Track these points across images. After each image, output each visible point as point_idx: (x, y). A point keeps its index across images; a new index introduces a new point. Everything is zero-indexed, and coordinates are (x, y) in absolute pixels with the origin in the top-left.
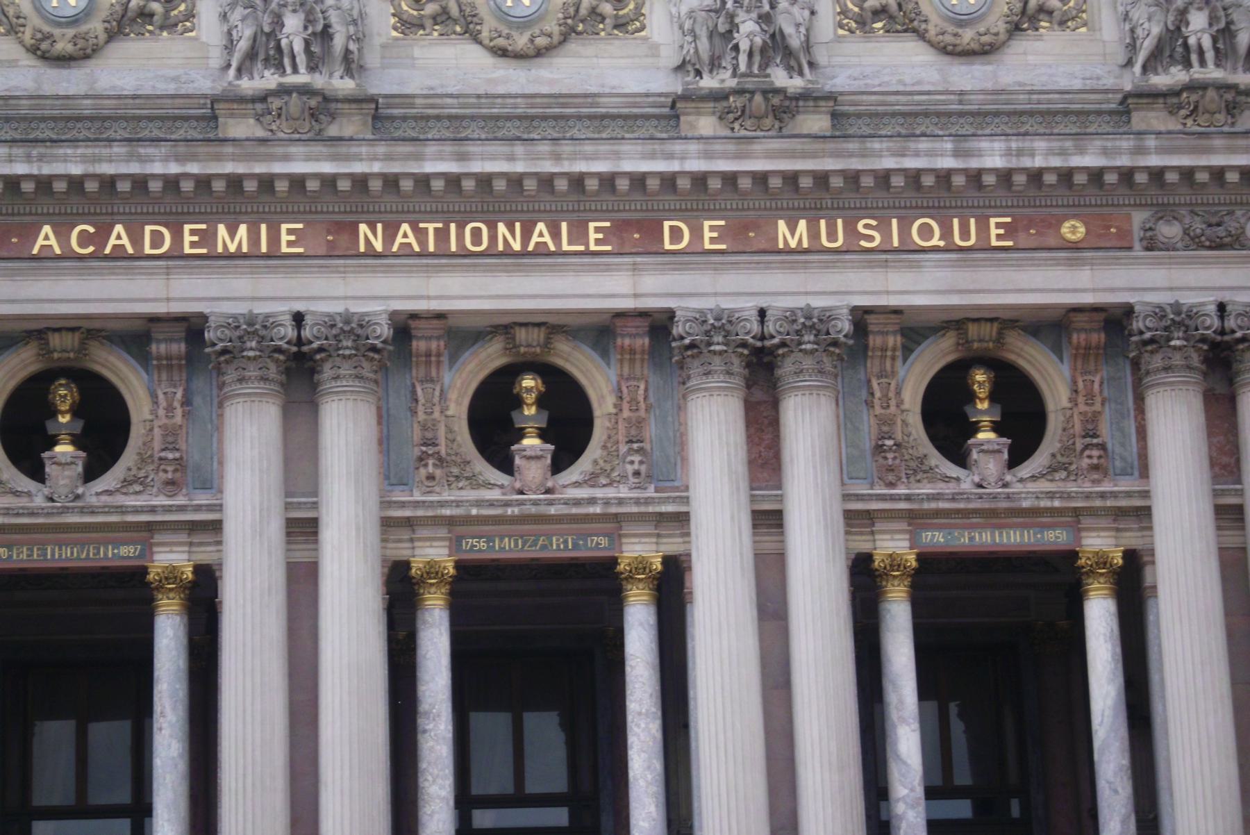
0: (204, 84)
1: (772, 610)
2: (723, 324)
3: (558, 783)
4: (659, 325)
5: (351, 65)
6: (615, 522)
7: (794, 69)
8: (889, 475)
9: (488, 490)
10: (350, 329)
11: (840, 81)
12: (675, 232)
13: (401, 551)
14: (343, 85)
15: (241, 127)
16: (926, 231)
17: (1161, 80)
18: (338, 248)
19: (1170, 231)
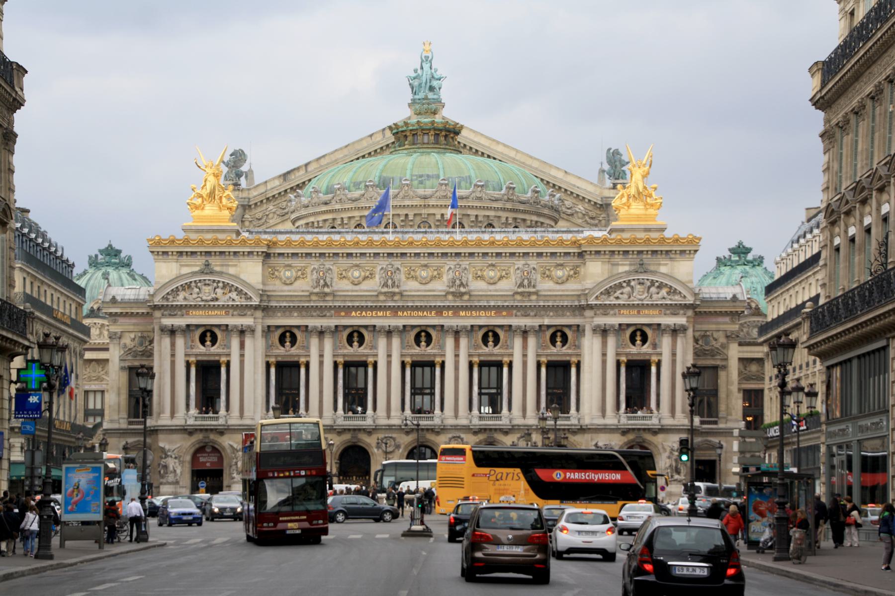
0: (376, 288)
1: (457, 368)
2: (452, 327)
3: (429, 386)
4: (442, 326)
5: (398, 287)
6: (435, 355)
7: (464, 287)
8: (476, 349)
9: (417, 350)
10: (397, 327)
11: (472, 288)
12: (445, 313)
13: (403, 359)
14: (396, 290)
15: (382, 298)
16: (482, 313)
17: (520, 290)
18: (395, 315)
19: (518, 314)
